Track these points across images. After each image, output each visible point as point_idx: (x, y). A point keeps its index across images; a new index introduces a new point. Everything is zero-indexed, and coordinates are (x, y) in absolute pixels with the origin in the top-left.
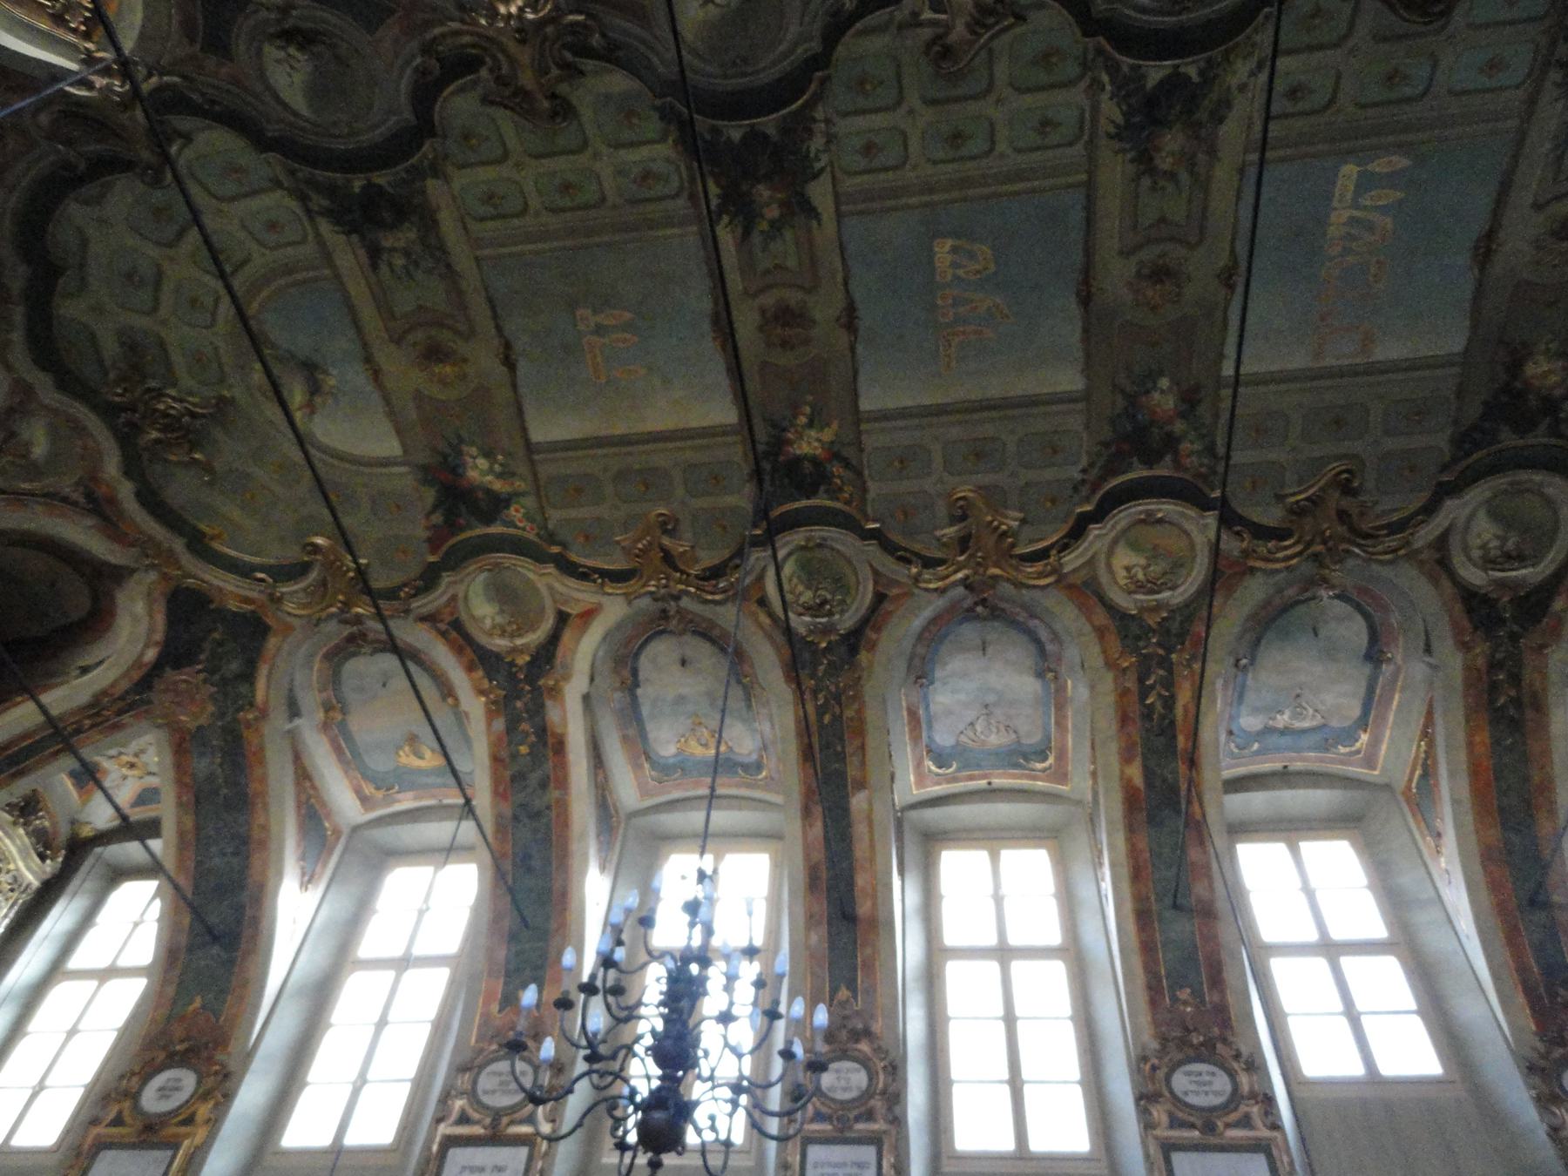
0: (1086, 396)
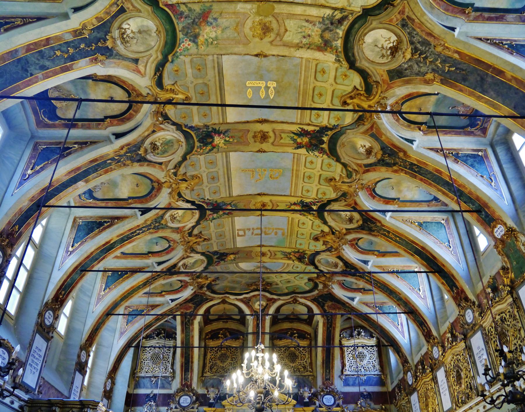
0: (230, 196)
